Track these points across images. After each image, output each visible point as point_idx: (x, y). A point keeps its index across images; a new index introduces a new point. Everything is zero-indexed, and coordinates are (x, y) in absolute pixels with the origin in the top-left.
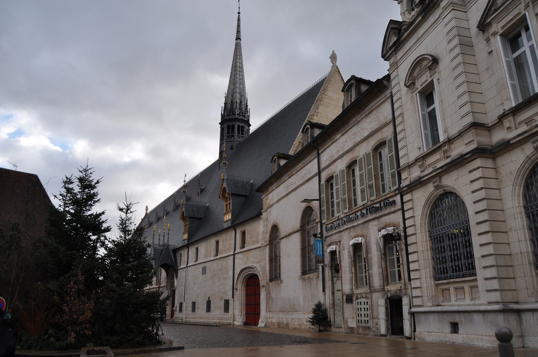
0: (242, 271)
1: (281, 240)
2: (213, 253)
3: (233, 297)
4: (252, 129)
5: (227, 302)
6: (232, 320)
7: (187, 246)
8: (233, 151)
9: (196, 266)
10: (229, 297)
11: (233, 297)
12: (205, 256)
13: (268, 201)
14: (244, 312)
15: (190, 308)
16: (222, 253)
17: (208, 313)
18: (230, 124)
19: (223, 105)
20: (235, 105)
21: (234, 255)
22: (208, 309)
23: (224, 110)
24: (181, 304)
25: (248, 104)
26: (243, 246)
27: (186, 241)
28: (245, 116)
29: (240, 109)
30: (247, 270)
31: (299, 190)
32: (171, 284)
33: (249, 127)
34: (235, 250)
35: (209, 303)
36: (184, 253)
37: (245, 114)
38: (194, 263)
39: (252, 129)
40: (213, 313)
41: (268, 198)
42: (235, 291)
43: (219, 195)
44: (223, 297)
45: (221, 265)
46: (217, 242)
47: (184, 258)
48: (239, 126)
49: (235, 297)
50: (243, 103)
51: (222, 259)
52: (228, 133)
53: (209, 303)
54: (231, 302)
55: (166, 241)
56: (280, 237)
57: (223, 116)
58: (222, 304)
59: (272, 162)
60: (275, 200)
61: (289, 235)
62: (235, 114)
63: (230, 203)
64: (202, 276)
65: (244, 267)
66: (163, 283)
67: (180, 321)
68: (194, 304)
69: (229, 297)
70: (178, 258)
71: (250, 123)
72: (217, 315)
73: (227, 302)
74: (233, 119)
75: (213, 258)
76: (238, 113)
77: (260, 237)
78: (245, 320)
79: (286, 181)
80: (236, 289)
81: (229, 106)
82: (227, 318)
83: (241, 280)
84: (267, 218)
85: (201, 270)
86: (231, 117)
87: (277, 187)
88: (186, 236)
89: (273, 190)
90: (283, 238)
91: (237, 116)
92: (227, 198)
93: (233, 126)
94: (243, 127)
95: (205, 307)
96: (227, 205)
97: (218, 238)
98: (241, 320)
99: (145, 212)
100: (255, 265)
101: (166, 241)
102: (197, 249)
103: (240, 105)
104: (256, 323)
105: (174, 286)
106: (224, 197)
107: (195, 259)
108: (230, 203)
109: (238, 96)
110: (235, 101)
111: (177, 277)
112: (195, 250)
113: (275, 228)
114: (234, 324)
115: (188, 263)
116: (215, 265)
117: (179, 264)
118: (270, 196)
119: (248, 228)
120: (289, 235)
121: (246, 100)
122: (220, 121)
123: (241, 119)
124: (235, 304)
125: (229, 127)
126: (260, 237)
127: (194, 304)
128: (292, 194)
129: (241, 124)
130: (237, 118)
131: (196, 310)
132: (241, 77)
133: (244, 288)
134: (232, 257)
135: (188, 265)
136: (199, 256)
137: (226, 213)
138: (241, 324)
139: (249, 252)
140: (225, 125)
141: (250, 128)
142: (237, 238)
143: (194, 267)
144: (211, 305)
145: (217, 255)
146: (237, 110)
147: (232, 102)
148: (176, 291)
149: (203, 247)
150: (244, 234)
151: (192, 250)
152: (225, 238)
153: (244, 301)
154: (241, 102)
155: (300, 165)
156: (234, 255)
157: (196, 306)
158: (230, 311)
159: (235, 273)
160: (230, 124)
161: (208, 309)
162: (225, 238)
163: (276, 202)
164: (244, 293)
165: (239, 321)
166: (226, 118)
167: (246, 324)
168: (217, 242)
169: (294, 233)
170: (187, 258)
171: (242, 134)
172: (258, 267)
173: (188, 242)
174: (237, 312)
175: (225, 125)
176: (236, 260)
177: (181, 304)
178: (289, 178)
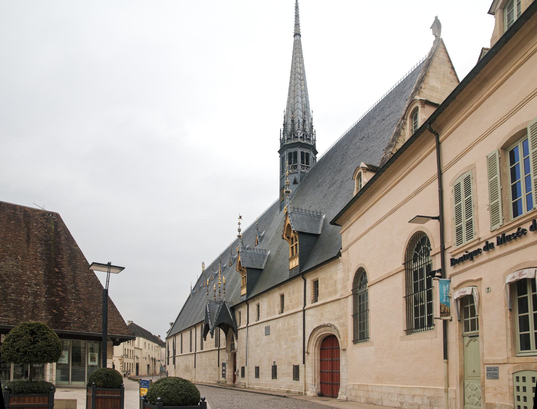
0: (315, 330)
2: (278, 309)
3: (304, 363)
5: (296, 369)
6: (304, 389)
7: (246, 302)
9: (258, 326)
10: (299, 362)
11: (304, 363)
12: (268, 314)
14: (318, 381)
15: (253, 374)
16: (288, 309)
17: (274, 380)
18: (292, 150)
19: (282, 127)
20: (297, 125)
21: (304, 311)
22: (274, 375)
23: (284, 134)
24: (243, 368)
25: (314, 124)
26: (316, 300)
27: (245, 296)
28: (309, 140)
29: (304, 130)
30: (322, 329)
32: (231, 347)
34: (305, 305)
35: (274, 368)
36: (243, 310)
37: (310, 136)
38: (256, 323)
40: (281, 380)
42: (306, 354)
43: (283, 236)
44: (291, 363)
45: (288, 324)
46: (282, 296)
47: (244, 317)
49: (306, 361)
50: (307, 122)
51: (289, 317)
53: (274, 368)
54: (301, 369)
57: (282, 141)
58: (291, 370)
62: (297, 137)
63: (296, 245)
64: (265, 337)
65: (317, 325)
66: (223, 344)
67: (243, 387)
68: (257, 369)
69: (299, 362)
70: (237, 317)
72: (285, 382)
73: (296, 369)
75: (278, 316)
76: (302, 135)
78: (319, 390)
80: (308, 353)
81: (289, 127)
82: (297, 387)
83: (313, 342)
85: (264, 330)
86: (293, 142)
88: (244, 291)
91: (299, 140)
92: (292, 239)
93: (296, 153)
95: (270, 373)
96: (292, 248)
97: (284, 290)
98: (315, 390)
102: (258, 306)
103: (303, 126)
104: (334, 395)
105: (234, 349)
106: (288, 238)
107: (256, 317)
108: (296, 245)
110: (296, 120)
111: (237, 339)
112: (255, 307)
114: (305, 394)
115: (248, 323)
116: (280, 324)
117: (238, 324)
121: (310, 118)
122: (279, 148)
123: (305, 144)
124: (307, 371)
125: (290, 154)
127: (257, 369)
130: (299, 143)
131: (260, 375)
133: (317, 351)
134: (302, 313)
135: (249, 325)
136: (260, 314)
138: (315, 394)
139: (324, 306)
142: (307, 289)
143: (255, 327)
144: (278, 371)
148: (237, 354)
150: (316, 283)
151: (253, 307)
152: (291, 291)
153: (318, 369)
154: (304, 121)
156: (304, 311)
157: (260, 372)
158: (300, 379)
159: (306, 334)
160: (292, 150)
161: (274, 375)
162: (291, 291)
164: (318, 357)
165: (312, 391)
166: (286, 143)
167: (321, 395)
168: (282, 296)
172: (336, 325)
173: (247, 297)
174: (310, 381)
176: (306, 317)
177: (243, 368)
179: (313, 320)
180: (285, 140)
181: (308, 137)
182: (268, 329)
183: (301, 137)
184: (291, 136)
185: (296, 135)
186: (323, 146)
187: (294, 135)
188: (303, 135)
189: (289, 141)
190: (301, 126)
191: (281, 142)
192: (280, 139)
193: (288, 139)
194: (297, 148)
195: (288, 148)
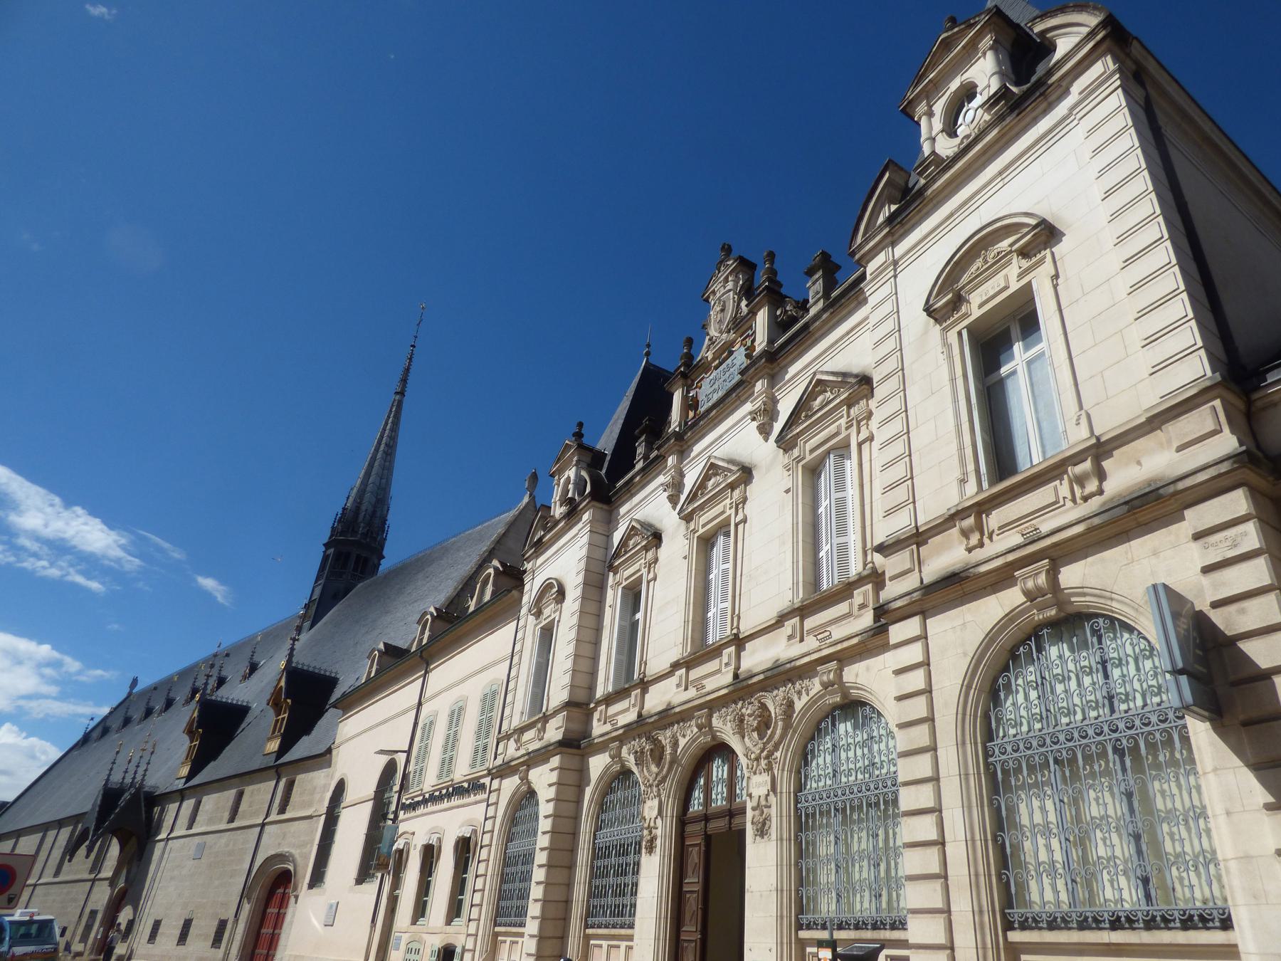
2: (226, 815)
21: (263, 825)
26: (282, 810)
34: (267, 815)
35: (187, 924)
48: (358, 557)
53: (187, 924)
54: (229, 926)
55: (139, 778)
68: (157, 925)
71: (385, 553)
73: (222, 925)
75: (223, 826)
94: (366, 560)
95: (177, 932)
99: (128, 690)
100: (293, 851)
101: (139, 778)
113: (340, 788)
122: (326, 540)
127: (157, 925)
137: (270, 739)
140: (331, 551)
141: (383, 561)
145: (231, 820)
151: (188, 804)
156: (263, 825)
170: (174, 817)
175: (331, 551)
182: (201, 848)
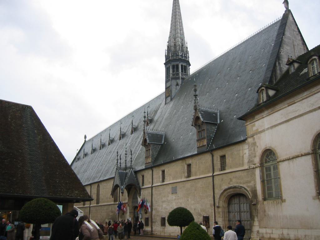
1: (280, 163)
4: (193, 70)
8: (178, 88)
13: (254, 128)
18: (175, 63)
20: (178, 47)
21: (213, 176)
26: (223, 168)
28: (186, 57)
29: (182, 51)
31: (305, 116)
33: (189, 67)
37: (187, 55)
39: (193, 70)
41: (254, 125)
48: (182, 66)
52: (173, 72)
56: (278, 160)
57: (167, 57)
59: (257, 92)
60: (266, 127)
61: (293, 158)
62: (178, 55)
74: (176, 59)
76: (181, 54)
77: (246, 161)
79: (283, 109)
81: (173, 49)
84: (254, 144)
87: (269, 115)
89: (263, 118)
90: (284, 161)
91: (180, 57)
93: (177, 66)
103: (182, 48)
107: (161, 179)
109: (180, 40)
110: (177, 44)
112: (161, 173)
116: (188, 185)
117: (141, 184)
118: (257, 123)
119: (227, 152)
120: (293, 158)
123: (184, 60)
125: (173, 67)
126: (246, 161)
128: (295, 120)
129: (184, 64)
130: (180, 59)
132: (181, 24)
141: (190, 67)
146: (180, 52)
147: (175, 45)
149: (169, 169)
150: (223, 157)
151: (158, 173)
154: (183, 45)
155: (305, 94)
160: (175, 63)
163: (268, 129)
168: (189, 166)
169: (302, 155)
170: (149, 180)
171: (185, 72)
178: (289, 106)
179: (223, 184)
180: (169, 57)
181: (185, 56)
183: (181, 55)
184: (174, 54)
185: (177, 54)
186: (196, 65)
187: (176, 53)
188: (182, 54)
189: (173, 57)
190: (181, 48)
191: (166, 57)
192: (166, 56)
193: (172, 56)
194: (179, 62)
195: (172, 62)
